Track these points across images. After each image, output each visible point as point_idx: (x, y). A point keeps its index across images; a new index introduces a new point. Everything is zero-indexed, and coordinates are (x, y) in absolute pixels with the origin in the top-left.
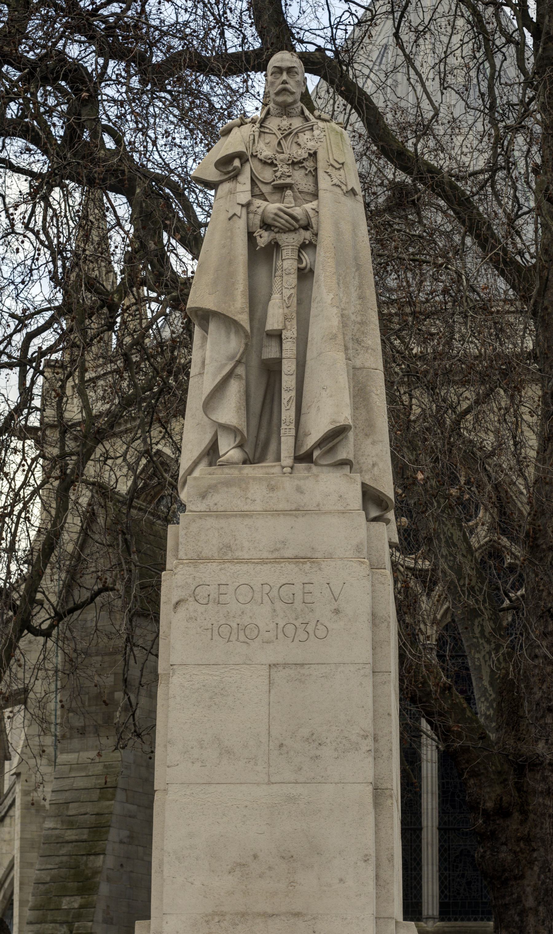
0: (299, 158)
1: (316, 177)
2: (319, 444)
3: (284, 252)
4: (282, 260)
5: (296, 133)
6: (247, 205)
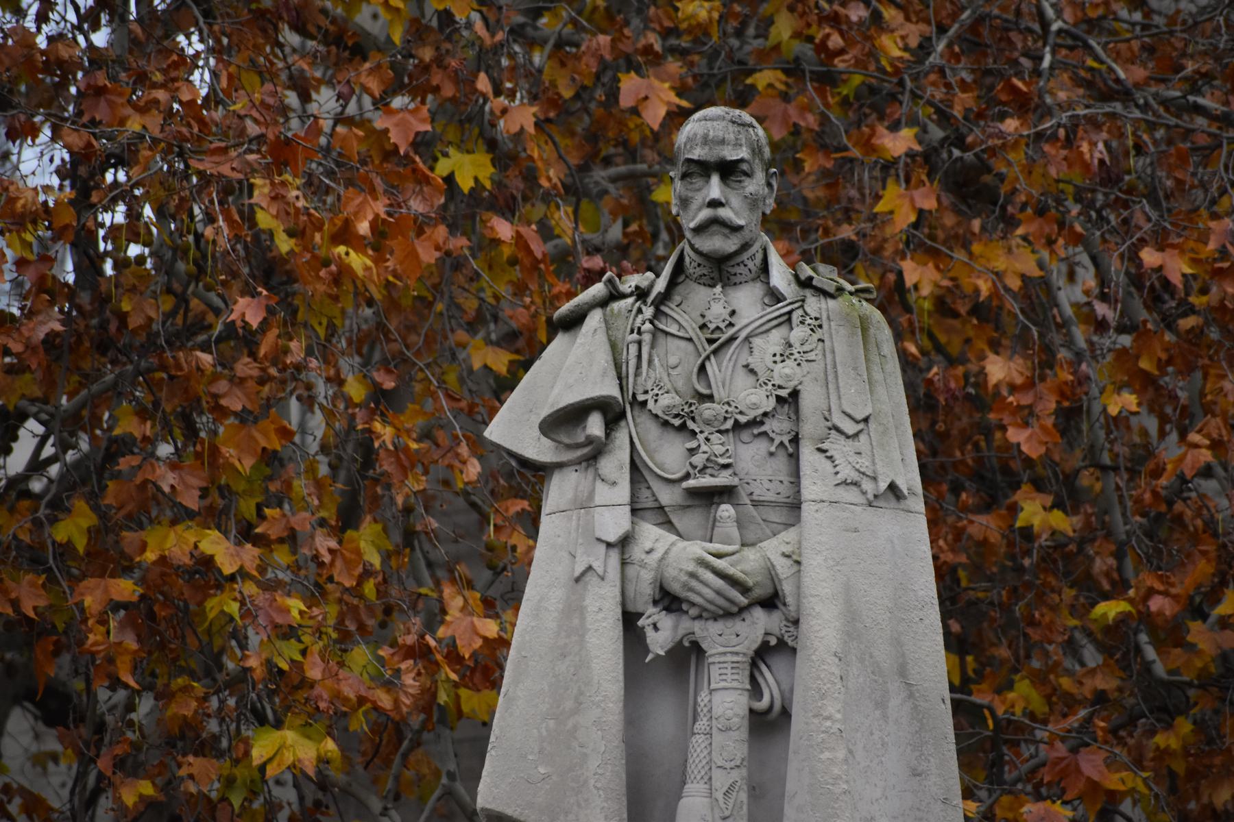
3: (715, 671)
4: (711, 692)
6: (625, 542)
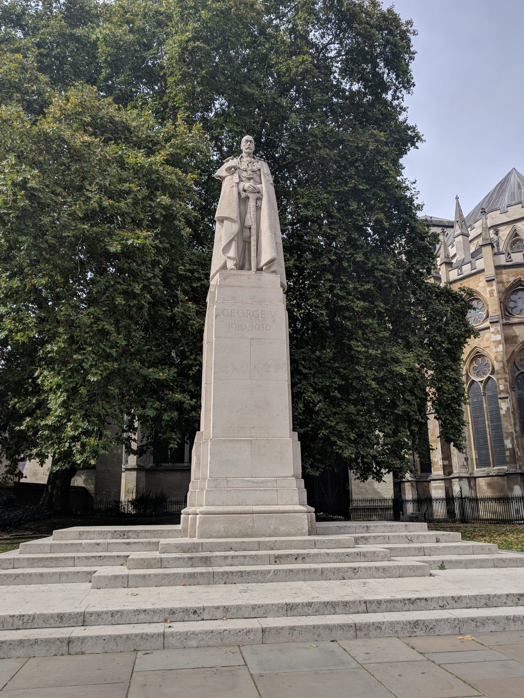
1: (260, 177)
2: (266, 264)
6: (238, 184)
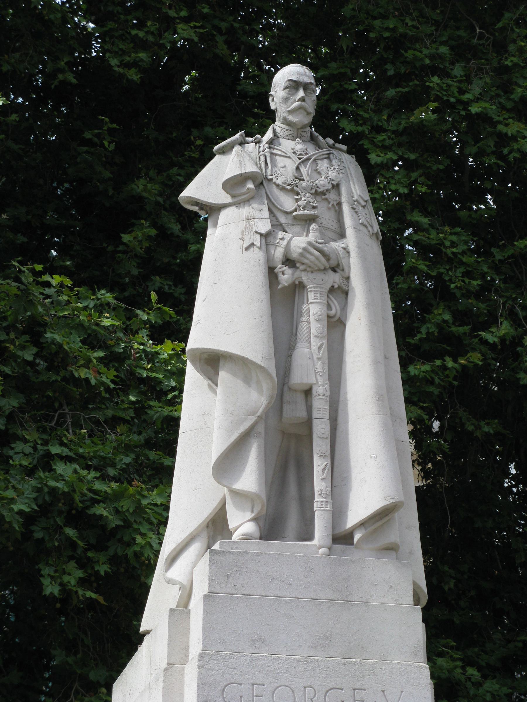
0: (323, 189)
5: (315, 160)
